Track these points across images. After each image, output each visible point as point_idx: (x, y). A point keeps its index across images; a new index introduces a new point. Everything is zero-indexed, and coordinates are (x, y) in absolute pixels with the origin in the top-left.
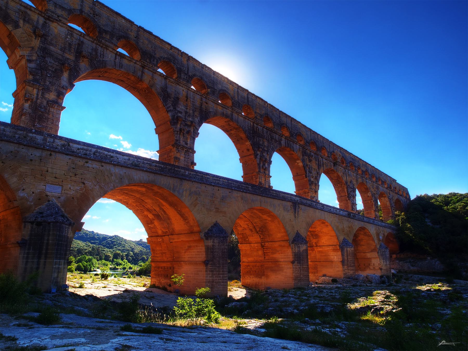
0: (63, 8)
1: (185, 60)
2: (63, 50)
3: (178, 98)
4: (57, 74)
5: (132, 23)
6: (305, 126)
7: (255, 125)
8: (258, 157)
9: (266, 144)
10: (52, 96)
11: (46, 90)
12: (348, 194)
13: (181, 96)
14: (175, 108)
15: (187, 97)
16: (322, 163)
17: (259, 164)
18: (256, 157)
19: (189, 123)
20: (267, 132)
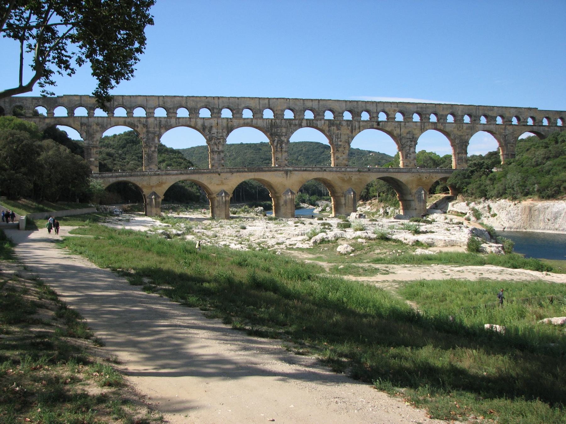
0: (151, 108)
1: (216, 101)
2: (154, 128)
3: (212, 127)
4: (153, 139)
5: (182, 97)
6: (338, 101)
7: (273, 121)
8: (276, 141)
9: (284, 130)
10: (153, 149)
11: (150, 147)
12: (402, 145)
13: (213, 125)
14: (210, 133)
15: (217, 124)
16: (357, 126)
17: (276, 146)
18: (274, 141)
19: (219, 138)
20: (285, 123)
